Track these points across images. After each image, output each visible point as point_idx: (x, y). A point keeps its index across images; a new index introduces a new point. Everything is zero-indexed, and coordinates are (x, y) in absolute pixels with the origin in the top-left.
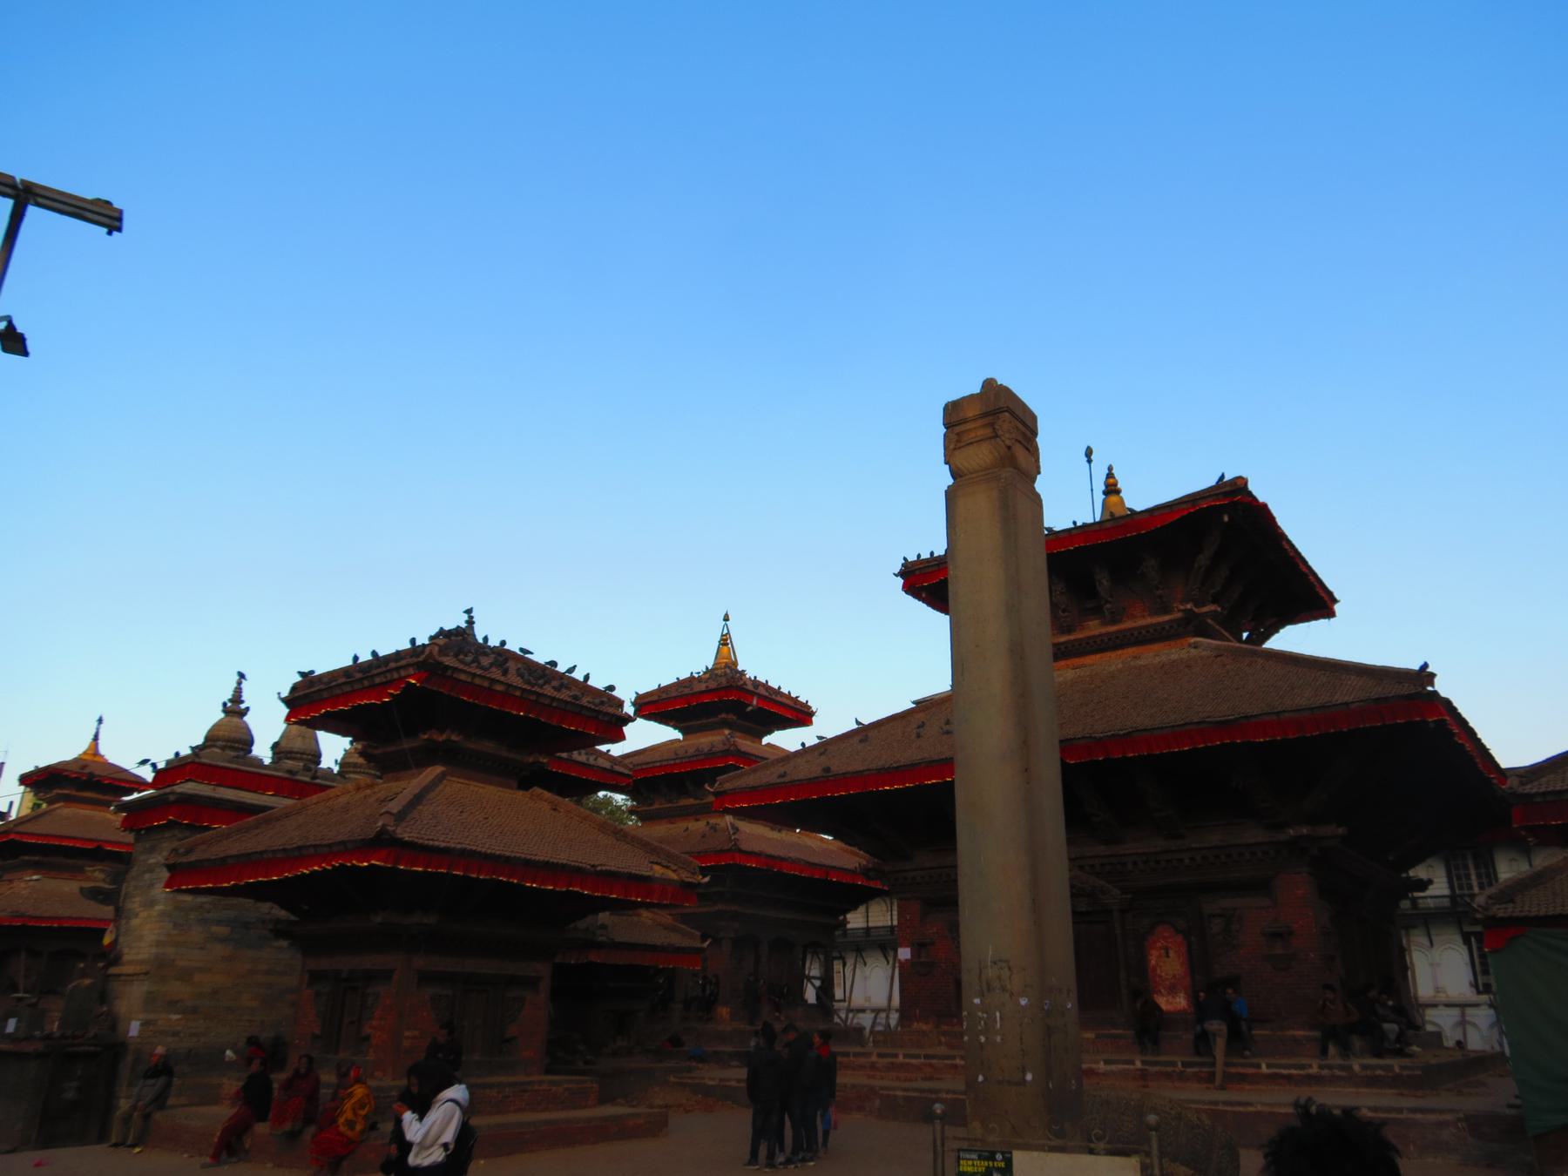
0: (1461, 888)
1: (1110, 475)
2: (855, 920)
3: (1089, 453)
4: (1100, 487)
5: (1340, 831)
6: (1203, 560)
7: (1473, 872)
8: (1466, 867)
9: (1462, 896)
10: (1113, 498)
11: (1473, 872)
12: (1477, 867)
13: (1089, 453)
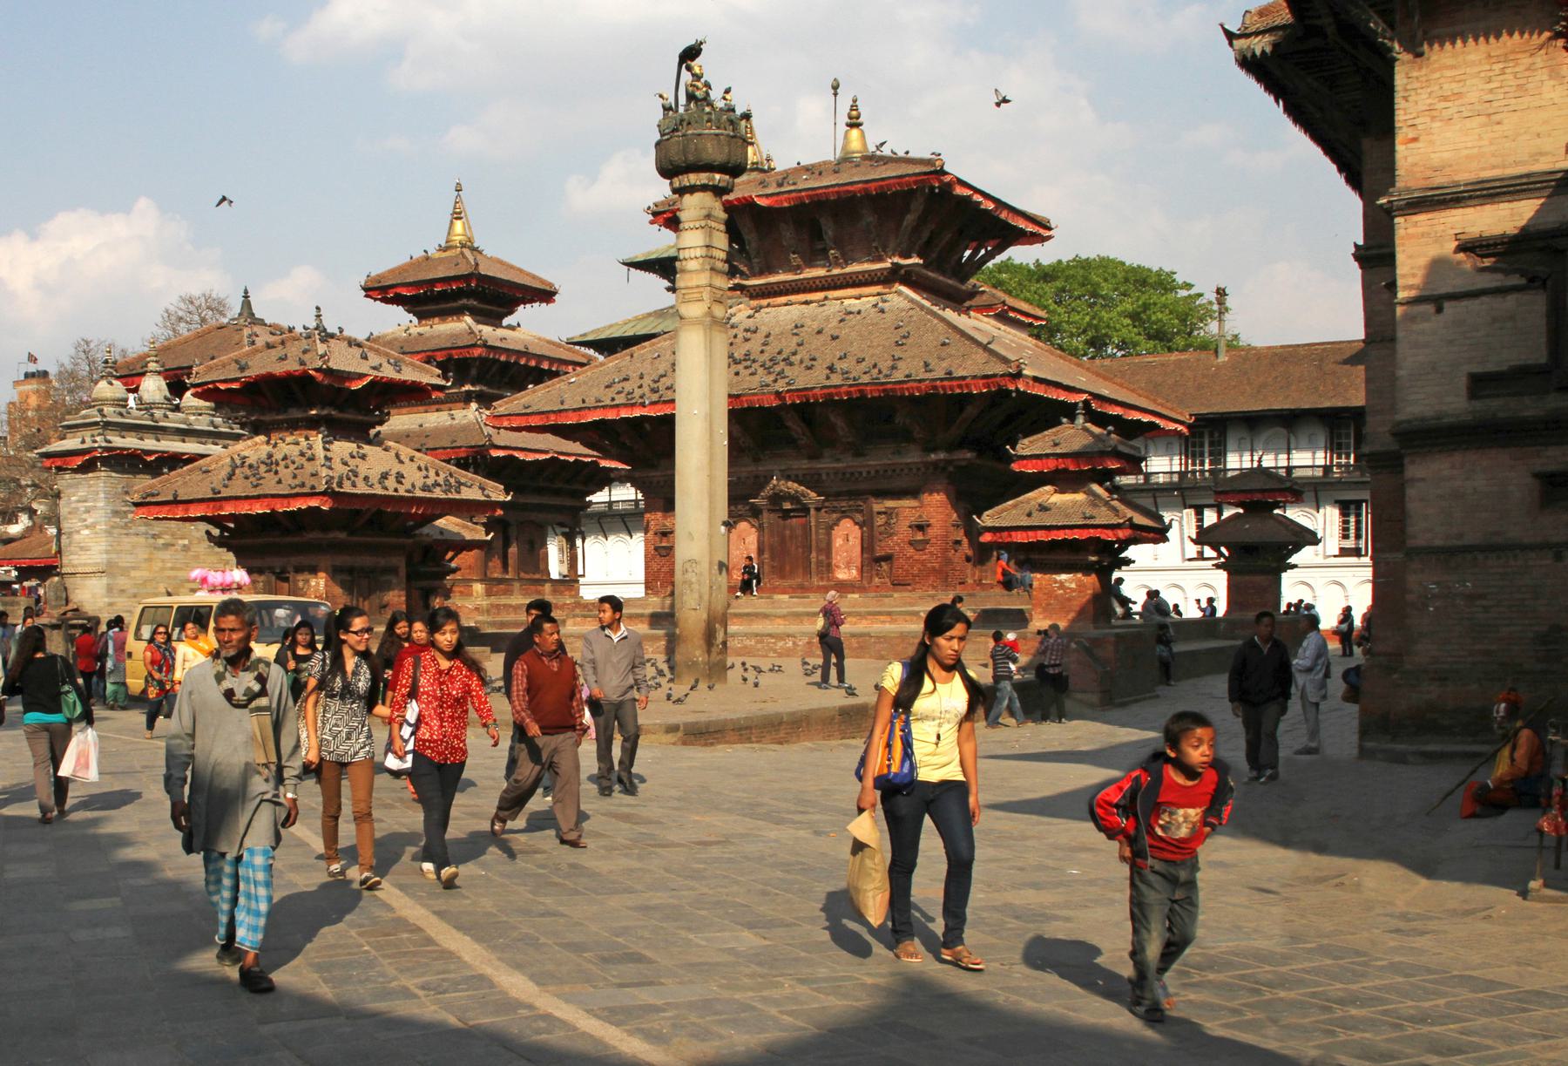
0: (1194, 464)
1: (854, 107)
2: (599, 497)
3: (835, 88)
4: (843, 119)
5: (969, 455)
6: (910, 219)
7: (1206, 449)
8: (1202, 445)
9: (1194, 472)
10: (855, 133)
11: (1206, 449)
12: (1211, 444)
13: (835, 88)
